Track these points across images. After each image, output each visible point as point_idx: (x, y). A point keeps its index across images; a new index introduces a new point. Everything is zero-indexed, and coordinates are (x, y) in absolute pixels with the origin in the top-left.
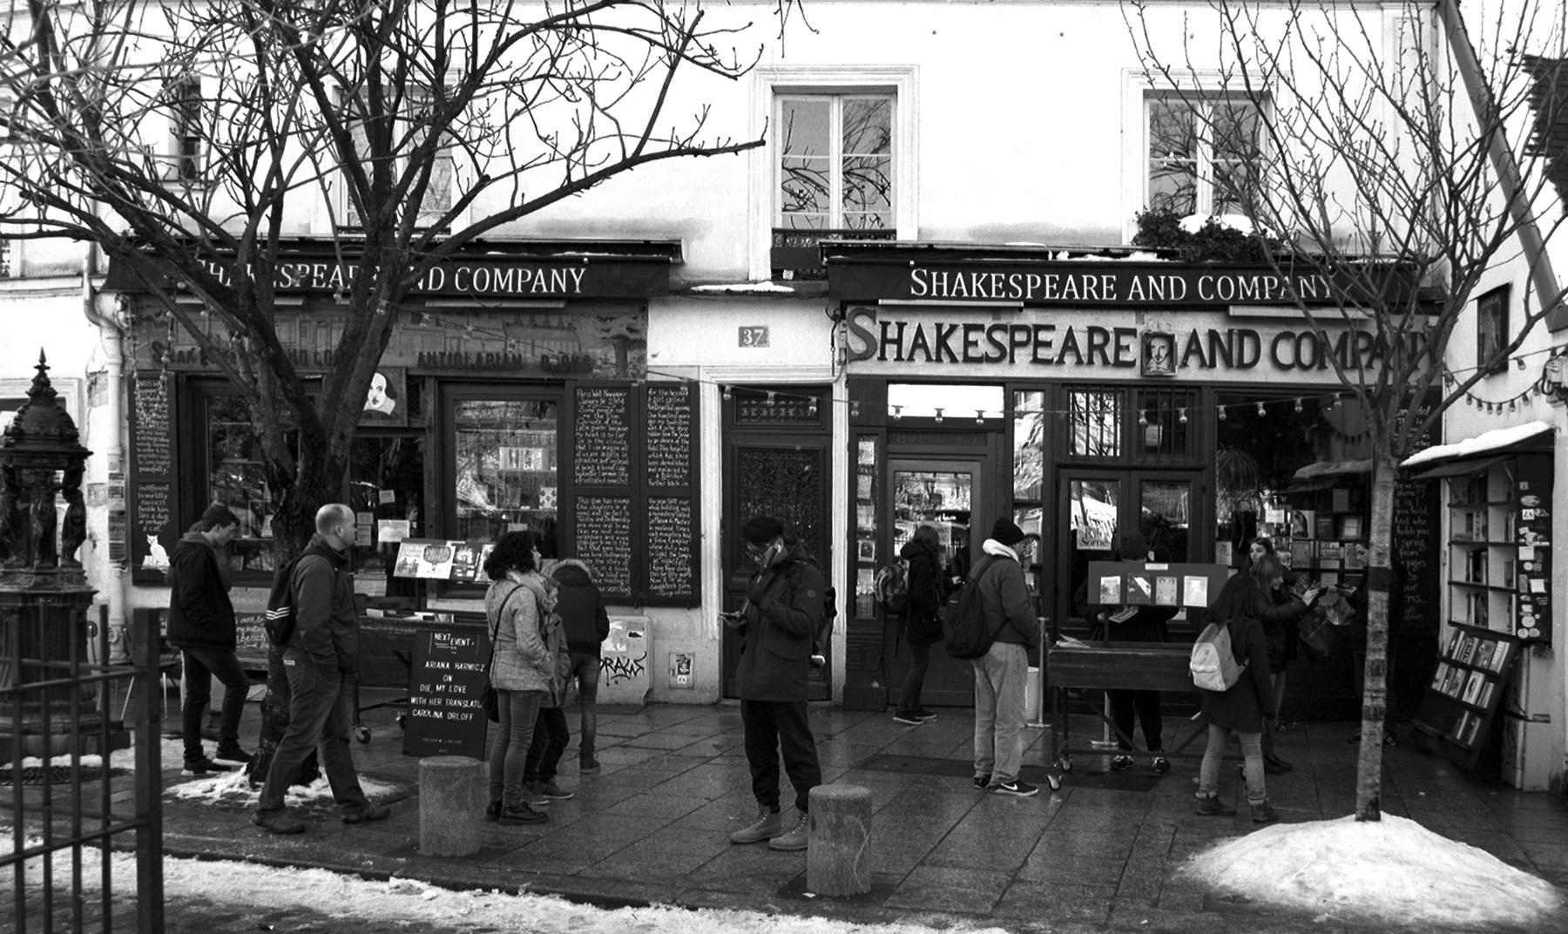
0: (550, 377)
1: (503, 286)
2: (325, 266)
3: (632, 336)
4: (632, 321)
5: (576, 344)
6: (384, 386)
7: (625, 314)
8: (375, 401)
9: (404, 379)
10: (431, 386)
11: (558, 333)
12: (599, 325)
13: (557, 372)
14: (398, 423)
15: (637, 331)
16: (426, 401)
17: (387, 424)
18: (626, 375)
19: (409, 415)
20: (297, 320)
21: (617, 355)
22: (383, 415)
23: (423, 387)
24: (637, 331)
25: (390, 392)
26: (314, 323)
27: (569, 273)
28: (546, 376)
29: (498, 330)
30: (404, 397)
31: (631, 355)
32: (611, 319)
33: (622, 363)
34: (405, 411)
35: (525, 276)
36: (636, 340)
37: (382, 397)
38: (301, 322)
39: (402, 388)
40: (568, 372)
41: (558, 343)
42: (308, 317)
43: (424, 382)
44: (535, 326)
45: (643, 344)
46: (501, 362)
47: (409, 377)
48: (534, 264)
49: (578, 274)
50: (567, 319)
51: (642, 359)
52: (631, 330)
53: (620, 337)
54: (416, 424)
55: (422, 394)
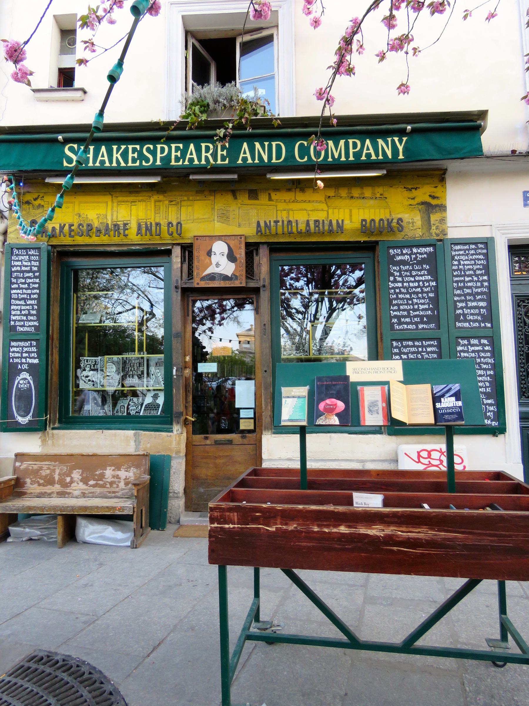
0: (366, 239)
1: (336, 156)
2: (181, 146)
3: (434, 202)
4: (434, 189)
5: (387, 211)
6: (226, 250)
7: (427, 184)
8: (218, 265)
9: (243, 246)
10: (264, 252)
11: (372, 202)
12: (406, 194)
13: (372, 233)
14: (237, 284)
15: (437, 198)
16: (259, 264)
17: (228, 284)
18: (431, 234)
19: (247, 278)
20: (153, 200)
21: (422, 218)
22: (225, 278)
23: (257, 254)
24: (437, 198)
25: (231, 257)
26: (167, 202)
27: (393, 142)
28: (362, 239)
29: (320, 202)
30: (243, 261)
31: (434, 218)
32: (416, 189)
33: (428, 224)
34: (244, 273)
35: (355, 145)
36: (437, 206)
37: (224, 261)
38: (156, 201)
39: (241, 254)
40: (381, 233)
41: (372, 211)
42: (161, 197)
43: (257, 250)
44: (352, 197)
45: (442, 208)
46: (326, 228)
47: (248, 245)
48: (362, 135)
49: (400, 141)
50: (379, 190)
51: (443, 220)
52: (433, 197)
53: (423, 203)
54: (252, 284)
55: (256, 259)
